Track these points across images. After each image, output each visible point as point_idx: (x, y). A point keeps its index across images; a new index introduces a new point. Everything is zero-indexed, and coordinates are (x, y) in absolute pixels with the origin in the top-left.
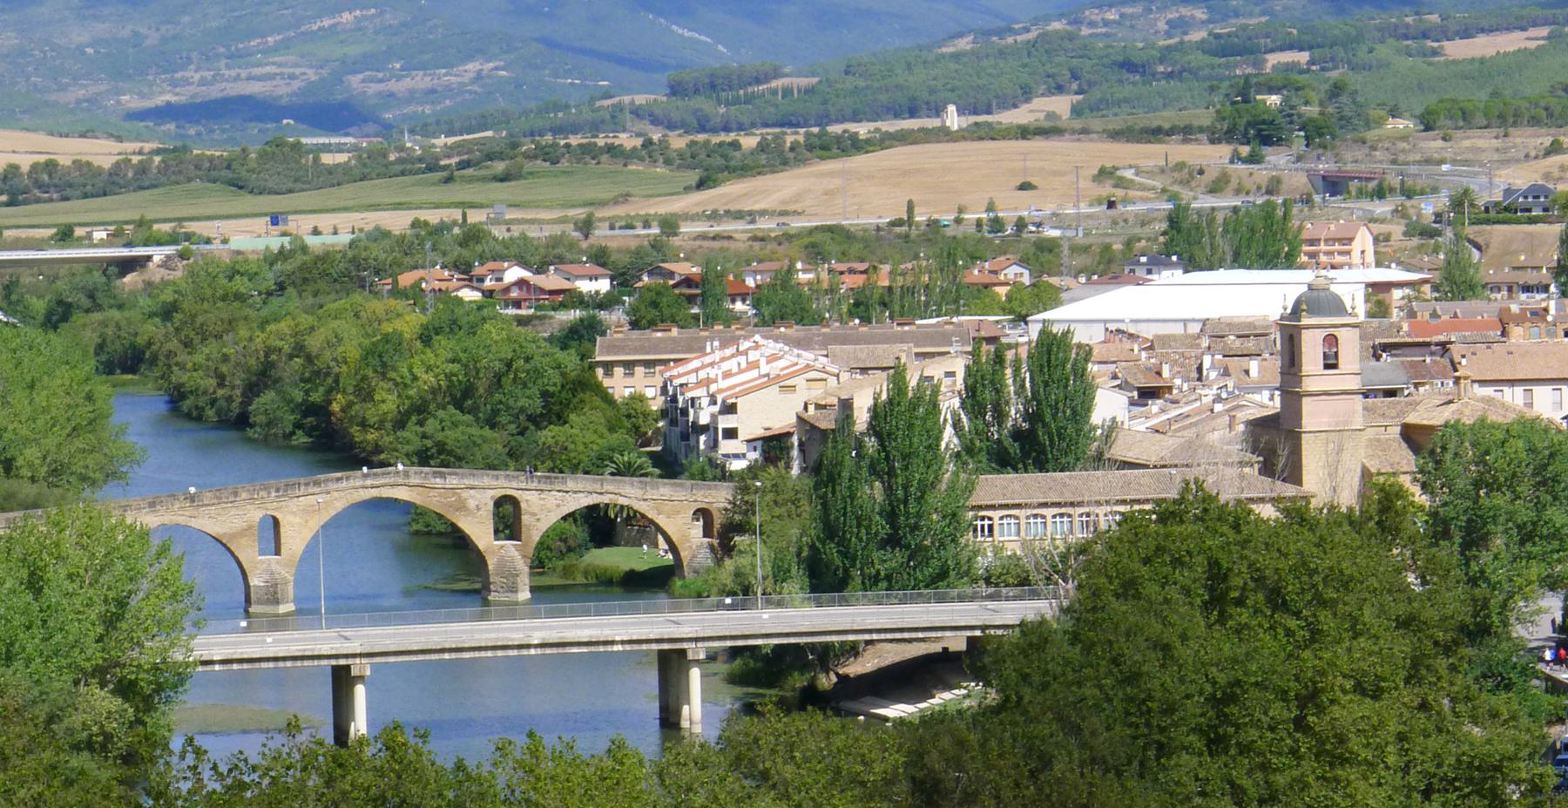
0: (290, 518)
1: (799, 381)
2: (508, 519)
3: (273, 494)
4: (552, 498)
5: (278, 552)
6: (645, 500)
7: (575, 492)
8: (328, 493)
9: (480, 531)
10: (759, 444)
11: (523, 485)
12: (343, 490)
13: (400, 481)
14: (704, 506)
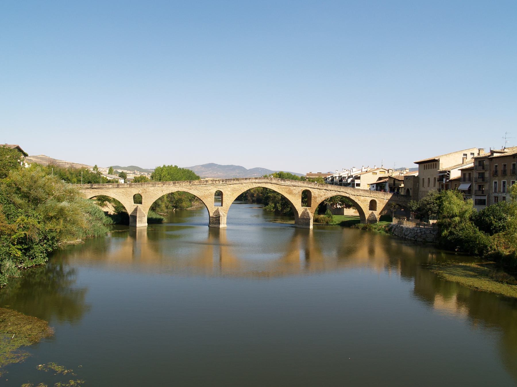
0: (227, 192)
1: (378, 171)
2: (306, 197)
3: (221, 182)
4: (322, 192)
5: (222, 206)
6: (354, 195)
7: (330, 191)
8: (242, 184)
9: (297, 202)
10: (375, 185)
11: (313, 187)
12: (248, 183)
13: (269, 181)
14: (374, 199)
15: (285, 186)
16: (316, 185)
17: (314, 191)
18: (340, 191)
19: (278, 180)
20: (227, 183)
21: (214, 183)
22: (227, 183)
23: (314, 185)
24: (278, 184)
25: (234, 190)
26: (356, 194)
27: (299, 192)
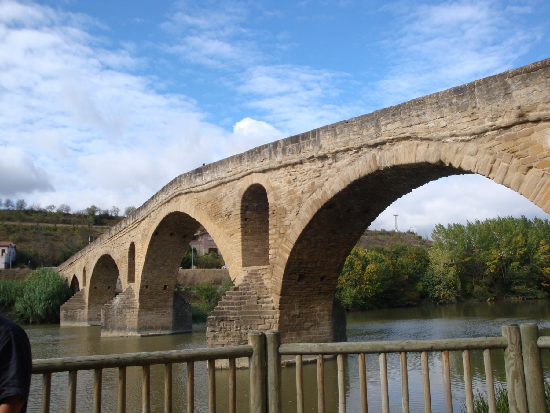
11: (266, 164)
15: (205, 192)
16: (276, 153)
17: (276, 184)
18: (378, 140)
19: (190, 179)
20: (137, 218)
21: (126, 226)
22: (137, 218)
23: (270, 155)
24: (192, 190)
25: (144, 236)
26: (488, 123)
27: (234, 205)
